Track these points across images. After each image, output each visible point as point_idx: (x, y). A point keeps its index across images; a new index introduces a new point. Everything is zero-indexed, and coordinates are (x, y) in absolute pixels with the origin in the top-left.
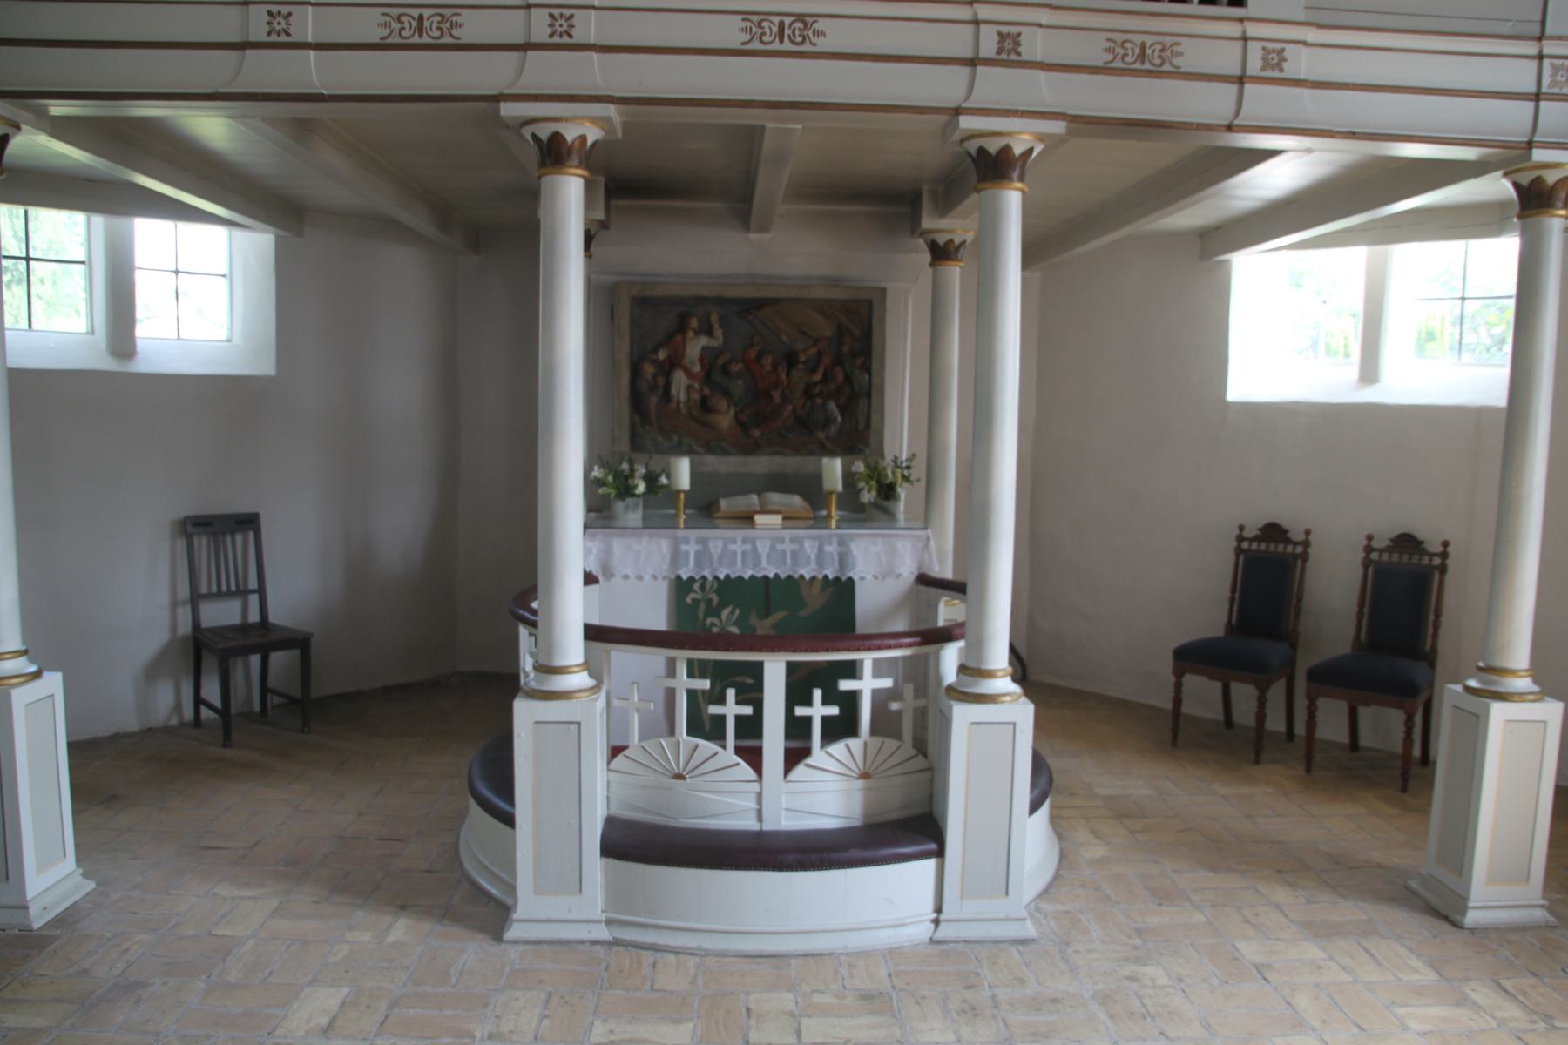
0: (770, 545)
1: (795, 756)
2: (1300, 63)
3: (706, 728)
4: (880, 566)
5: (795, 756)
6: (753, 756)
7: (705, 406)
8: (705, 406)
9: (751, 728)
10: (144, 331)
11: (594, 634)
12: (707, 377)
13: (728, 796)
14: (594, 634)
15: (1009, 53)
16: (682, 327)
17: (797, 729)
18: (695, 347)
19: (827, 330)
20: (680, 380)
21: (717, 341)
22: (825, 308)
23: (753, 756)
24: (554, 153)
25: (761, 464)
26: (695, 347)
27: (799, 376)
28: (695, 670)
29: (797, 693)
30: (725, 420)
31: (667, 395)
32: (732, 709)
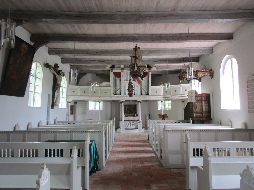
0: (132, 118)
1: (132, 125)
2: (151, 97)
3: (129, 124)
4: (136, 118)
5: (132, 125)
6: (130, 125)
7: (127, 111)
8: (127, 111)
9: (130, 124)
10: (96, 108)
11: (124, 121)
12: (128, 110)
13: (130, 127)
14: (124, 121)
15: (139, 98)
16: (126, 107)
17: (132, 124)
18: (127, 108)
19: (134, 107)
20: (126, 110)
21: (128, 107)
22: (134, 105)
23: (130, 125)
24: (122, 102)
25: (131, 114)
26: (127, 108)
27: (132, 109)
28: (128, 122)
29: (132, 123)
30: (128, 112)
31: (125, 110)
32: (130, 123)
